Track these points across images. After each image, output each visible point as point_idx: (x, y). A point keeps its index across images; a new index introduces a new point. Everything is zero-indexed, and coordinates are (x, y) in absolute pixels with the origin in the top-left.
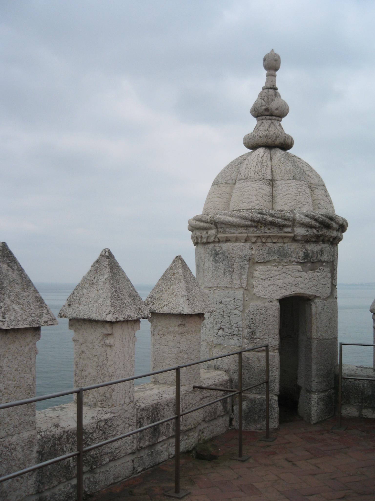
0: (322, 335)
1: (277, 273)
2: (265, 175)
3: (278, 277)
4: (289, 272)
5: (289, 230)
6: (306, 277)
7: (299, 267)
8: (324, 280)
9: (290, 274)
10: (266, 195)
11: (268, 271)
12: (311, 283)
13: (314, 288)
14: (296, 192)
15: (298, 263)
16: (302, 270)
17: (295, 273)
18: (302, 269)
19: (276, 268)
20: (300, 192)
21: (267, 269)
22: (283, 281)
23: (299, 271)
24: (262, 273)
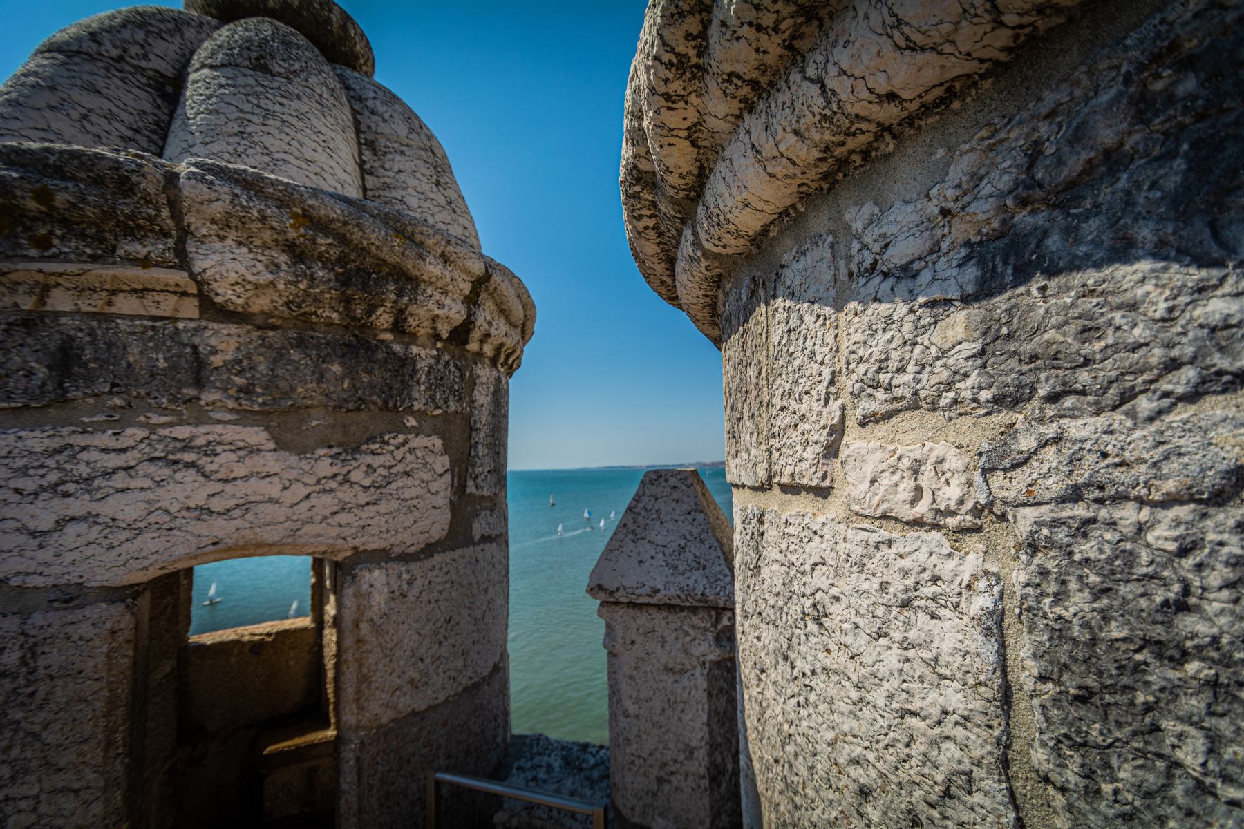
0: (386, 706)
1: (114, 461)
2: (135, 50)
3: (119, 480)
4: (189, 457)
5: (155, 248)
6: (293, 474)
7: (255, 435)
8: (409, 482)
9: (192, 465)
10: (110, 117)
11: (59, 451)
12: (325, 503)
13: (343, 518)
14: (247, 107)
15: (244, 417)
16: (272, 445)
17: (226, 458)
18: (274, 438)
19: (106, 439)
20: (268, 114)
21: (56, 443)
22: (149, 495)
23: (255, 450)
24: (19, 463)
